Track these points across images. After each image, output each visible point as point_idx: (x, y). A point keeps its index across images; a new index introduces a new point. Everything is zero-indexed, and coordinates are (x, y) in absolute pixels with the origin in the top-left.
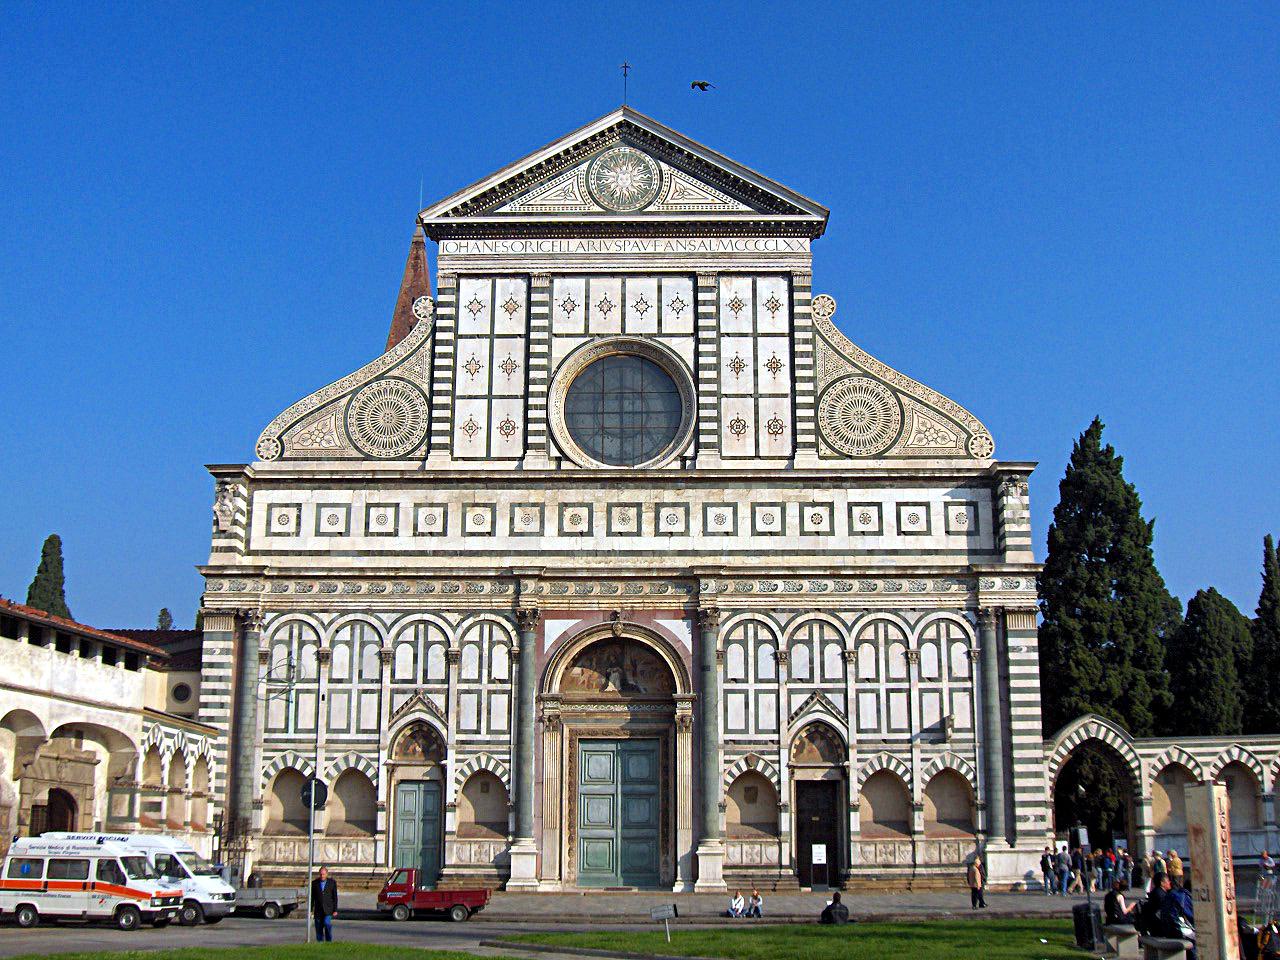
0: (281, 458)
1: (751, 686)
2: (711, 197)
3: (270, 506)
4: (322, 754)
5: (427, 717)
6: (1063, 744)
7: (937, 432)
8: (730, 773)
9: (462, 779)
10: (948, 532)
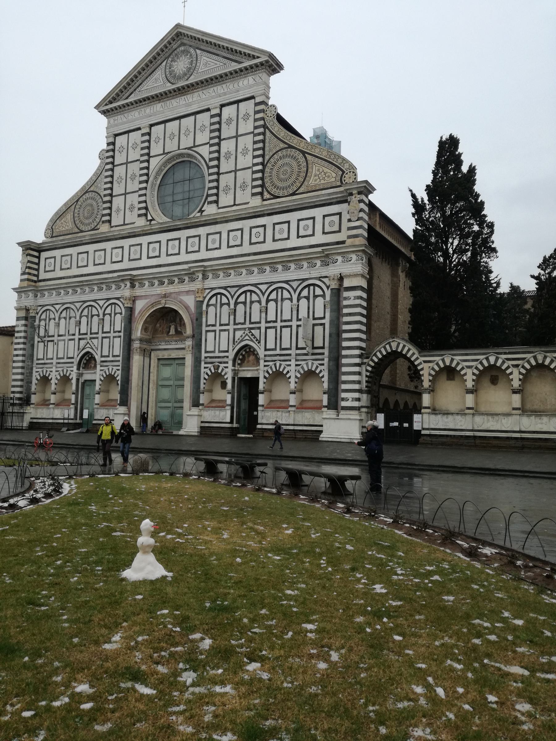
0: (52, 237)
1: (218, 328)
2: (219, 63)
3: (46, 259)
4: (54, 369)
5: (91, 350)
6: (375, 355)
7: (325, 174)
8: (207, 374)
9: (102, 379)
10: (324, 233)
